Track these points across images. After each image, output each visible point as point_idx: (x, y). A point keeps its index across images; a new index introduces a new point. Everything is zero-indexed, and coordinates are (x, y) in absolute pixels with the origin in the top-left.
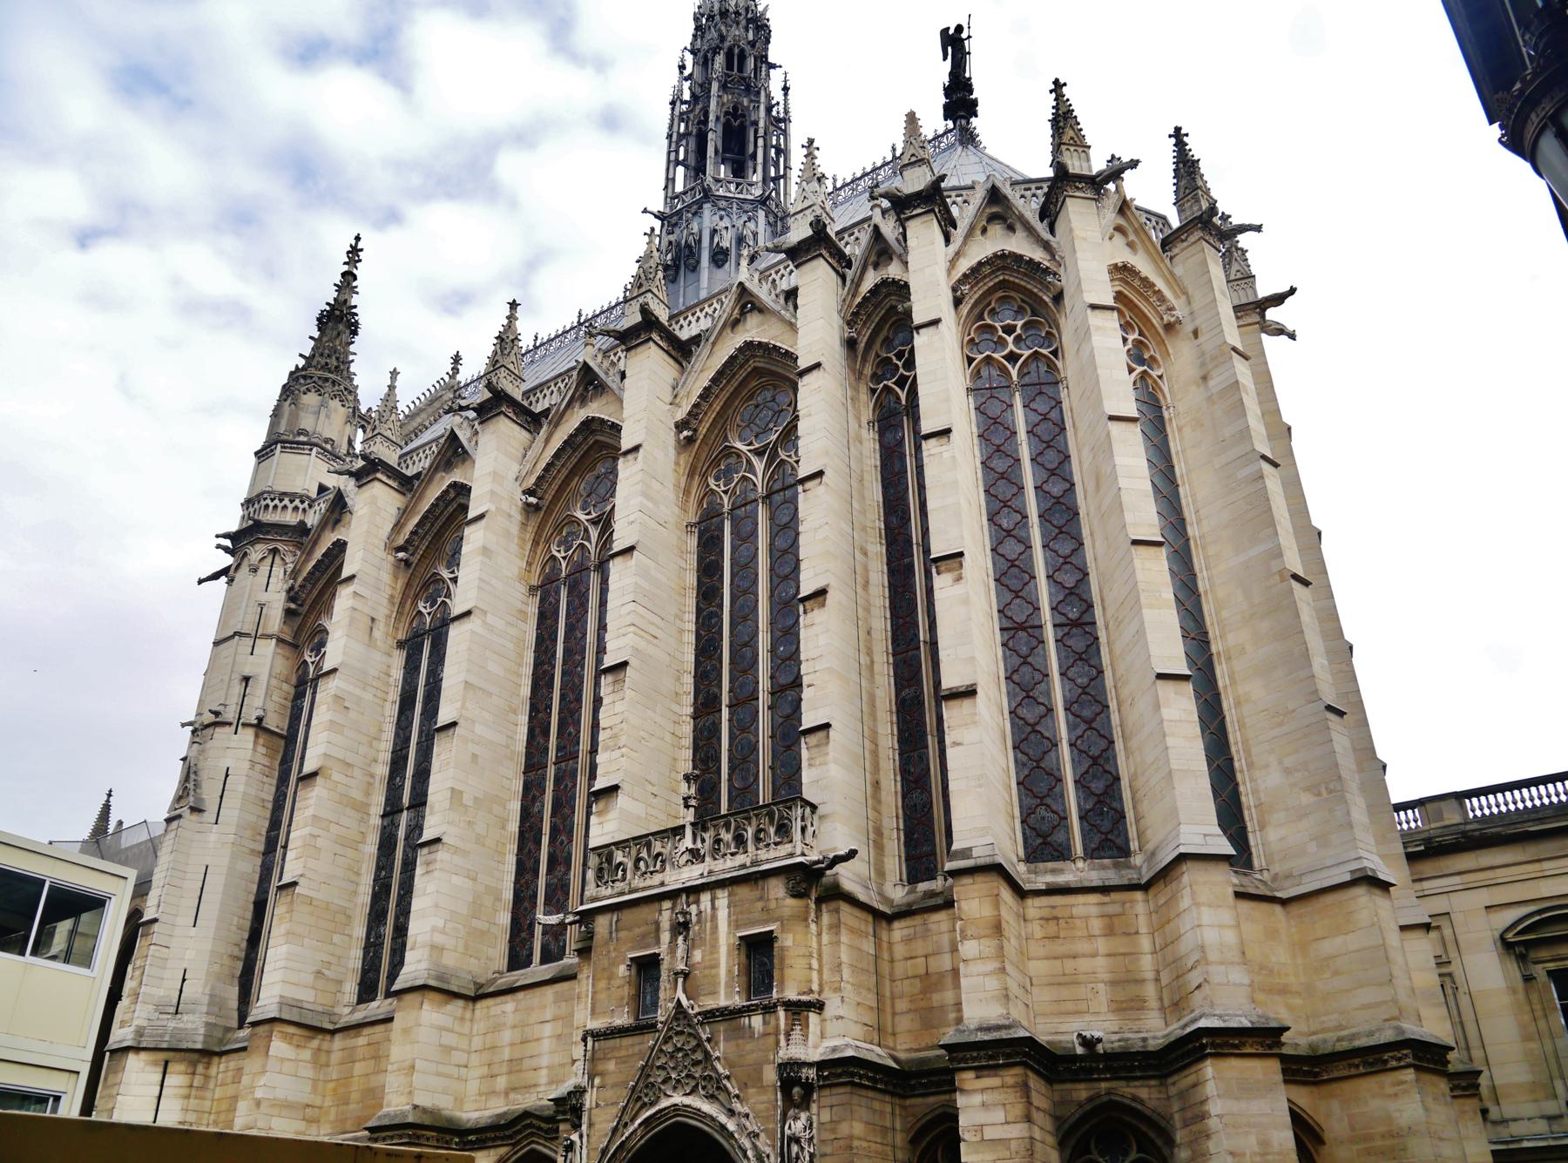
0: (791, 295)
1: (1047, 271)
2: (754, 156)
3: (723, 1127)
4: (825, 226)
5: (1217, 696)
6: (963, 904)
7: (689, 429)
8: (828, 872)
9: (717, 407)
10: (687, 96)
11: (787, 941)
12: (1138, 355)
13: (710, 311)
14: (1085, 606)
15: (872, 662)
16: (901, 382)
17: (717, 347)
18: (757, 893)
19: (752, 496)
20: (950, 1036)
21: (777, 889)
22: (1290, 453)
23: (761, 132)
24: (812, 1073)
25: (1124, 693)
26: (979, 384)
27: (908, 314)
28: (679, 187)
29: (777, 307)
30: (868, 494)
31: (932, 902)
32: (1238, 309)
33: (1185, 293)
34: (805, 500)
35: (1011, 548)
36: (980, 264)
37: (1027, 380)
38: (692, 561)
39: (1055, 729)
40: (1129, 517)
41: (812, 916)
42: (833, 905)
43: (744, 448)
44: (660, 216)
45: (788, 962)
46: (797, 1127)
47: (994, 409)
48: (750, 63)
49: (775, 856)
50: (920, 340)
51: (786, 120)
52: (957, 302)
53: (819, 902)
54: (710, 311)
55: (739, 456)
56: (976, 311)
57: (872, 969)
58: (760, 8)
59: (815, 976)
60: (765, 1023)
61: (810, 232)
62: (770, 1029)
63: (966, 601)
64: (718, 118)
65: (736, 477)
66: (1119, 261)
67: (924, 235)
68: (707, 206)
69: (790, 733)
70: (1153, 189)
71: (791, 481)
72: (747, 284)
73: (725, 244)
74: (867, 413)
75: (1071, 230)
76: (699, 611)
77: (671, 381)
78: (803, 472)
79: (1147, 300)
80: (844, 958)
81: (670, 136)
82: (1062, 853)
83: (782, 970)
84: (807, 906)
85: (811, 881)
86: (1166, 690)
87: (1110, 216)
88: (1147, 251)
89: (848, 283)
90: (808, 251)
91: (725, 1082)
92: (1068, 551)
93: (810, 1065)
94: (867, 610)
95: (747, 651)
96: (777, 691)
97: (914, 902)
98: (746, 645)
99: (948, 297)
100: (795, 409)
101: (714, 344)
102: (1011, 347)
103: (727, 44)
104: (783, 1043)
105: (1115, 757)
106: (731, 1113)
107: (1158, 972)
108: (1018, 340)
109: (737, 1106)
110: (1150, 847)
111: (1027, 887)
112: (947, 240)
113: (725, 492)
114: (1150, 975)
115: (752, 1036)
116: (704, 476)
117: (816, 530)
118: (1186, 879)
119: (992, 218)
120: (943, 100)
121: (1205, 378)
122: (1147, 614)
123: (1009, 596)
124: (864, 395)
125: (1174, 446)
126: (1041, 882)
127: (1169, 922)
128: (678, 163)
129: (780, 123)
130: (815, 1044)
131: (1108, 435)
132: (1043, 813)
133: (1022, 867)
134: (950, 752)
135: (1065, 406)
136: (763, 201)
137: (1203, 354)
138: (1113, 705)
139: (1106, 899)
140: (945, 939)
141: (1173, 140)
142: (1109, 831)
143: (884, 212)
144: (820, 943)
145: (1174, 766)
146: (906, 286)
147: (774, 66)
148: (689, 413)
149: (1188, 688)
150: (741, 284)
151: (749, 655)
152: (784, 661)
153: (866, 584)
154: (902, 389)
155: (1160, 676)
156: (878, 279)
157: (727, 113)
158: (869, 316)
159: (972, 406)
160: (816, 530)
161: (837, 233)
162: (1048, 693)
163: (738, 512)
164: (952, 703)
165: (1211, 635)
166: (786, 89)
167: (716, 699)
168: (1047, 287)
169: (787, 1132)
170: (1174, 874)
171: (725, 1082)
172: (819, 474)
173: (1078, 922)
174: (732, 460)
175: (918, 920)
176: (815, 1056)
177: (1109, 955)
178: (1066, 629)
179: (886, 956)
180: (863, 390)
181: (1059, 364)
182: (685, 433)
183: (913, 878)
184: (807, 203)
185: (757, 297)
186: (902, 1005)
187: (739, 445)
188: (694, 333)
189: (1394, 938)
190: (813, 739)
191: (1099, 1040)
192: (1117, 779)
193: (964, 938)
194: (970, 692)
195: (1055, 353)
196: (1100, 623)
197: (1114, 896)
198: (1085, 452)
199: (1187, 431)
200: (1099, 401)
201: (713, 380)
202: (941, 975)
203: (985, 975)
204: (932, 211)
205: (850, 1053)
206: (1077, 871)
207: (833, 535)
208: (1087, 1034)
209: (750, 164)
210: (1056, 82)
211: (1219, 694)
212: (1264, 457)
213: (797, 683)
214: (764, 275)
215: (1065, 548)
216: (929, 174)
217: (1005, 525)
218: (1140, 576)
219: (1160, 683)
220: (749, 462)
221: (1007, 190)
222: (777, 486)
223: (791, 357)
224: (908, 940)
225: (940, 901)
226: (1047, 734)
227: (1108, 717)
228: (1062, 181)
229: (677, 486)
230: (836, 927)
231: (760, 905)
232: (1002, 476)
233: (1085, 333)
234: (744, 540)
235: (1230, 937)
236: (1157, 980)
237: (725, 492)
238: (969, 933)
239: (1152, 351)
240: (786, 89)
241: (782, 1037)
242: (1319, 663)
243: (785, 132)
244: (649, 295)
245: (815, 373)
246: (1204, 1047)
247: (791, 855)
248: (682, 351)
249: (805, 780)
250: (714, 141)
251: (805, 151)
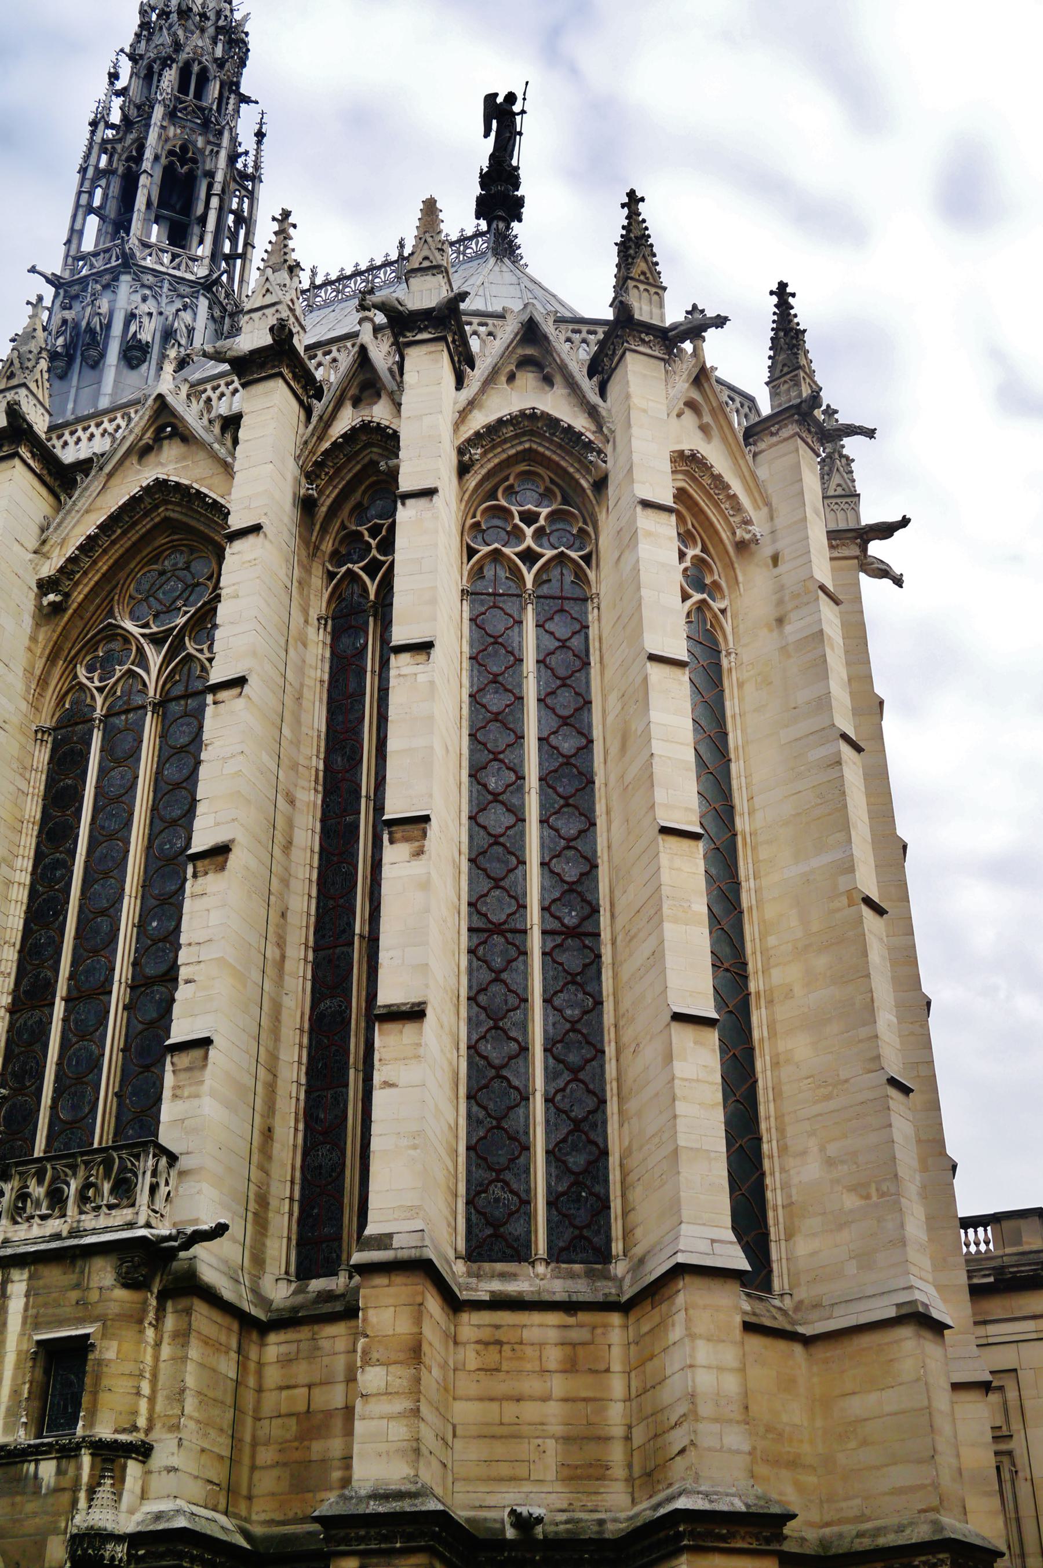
0: (232, 423)
1: (589, 446)
2: (203, 220)
4: (291, 334)
5: (749, 1052)
6: (371, 1313)
7: (57, 592)
8: (182, 1254)
9: (103, 566)
10: (115, 118)
11: (109, 1351)
12: (697, 578)
13: (110, 428)
14: (587, 910)
15: (283, 957)
16: (372, 569)
17: (113, 482)
18: (72, 1278)
19: (139, 701)
20: (329, 1504)
21: (103, 1274)
22: (878, 736)
23: (217, 188)
24: (120, 1551)
25: (627, 1036)
26: (480, 587)
27: (393, 474)
28: (88, 245)
29: (208, 438)
30: (305, 718)
31: (327, 1308)
32: (833, 536)
33: (768, 504)
34: (216, 715)
35: (497, 819)
36: (500, 422)
37: (545, 590)
38: (39, 781)
39: (527, 1077)
40: (660, 795)
41: (151, 1316)
42: (183, 1303)
43: (136, 631)
44: (54, 281)
45: (105, 1382)
47: (497, 624)
48: (214, 90)
49: (105, 1225)
50: (406, 514)
51: (255, 178)
52: (463, 470)
53: (163, 1297)
54: (110, 428)
55: (126, 641)
56: (488, 486)
57: (229, 1400)
58: (238, 16)
59: (143, 1405)
60: (60, 1472)
61: (267, 340)
62: (66, 1482)
63: (425, 885)
64: (157, 158)
65: (119, 670)
66: (686, 447)
67: (427, 370)
68: (125, 278)
69: (151, 1048)
70: (740, 359)
71: (199, 686)
72: (170, 399)
73: (145, 336)
74: (319, 605)
75: (628, 396)
76: (39, 856)
77: (39, 519)
78: (216, 676)
79: (717, 505)
80: (190, 1381)
81: (83, 170)
82: (519, 1252)
83: (95, 1394)
84: (145, 1302)
85: (158, 1269)
86: (683, 1036)
87: (682, 386)
88: (724, 439)
89: (314, 420)
90: (262, 366)
92: (573, 832)
93: (119, 1538)
94: (285, 882)
95: (104, 923)
96: (138, 985)
97: (301, 1307)
98: (103, 912)
99: (449, 461)
100: (217, 586)
101: (110, 475)
102: (529, 542)
103: (183, 56)
104: (82, 1503)
105: (605, 1122)
107: (630, 1427)
108: (539, 534)
110: (638, 1251)
111: (464, 1295)
112: (460, 384)
113: (100, 690)
114: (619, 1431)
115: (37, 1491)
116: (72, 663)
117: (225, 760)
118: (680, 1299)
119: (525, 363)
120: (478, 191)
121: (780, 621)
122: (670, 930)
123: (485, 885)
124: (317, 580)
125: (731, 707)
126: (485, 1289)
127: (651, 1358)
128: (90, 210)
129: (246, 181)
131: (645, 679)
132: (498, 1192)
133: (460, 1267)
134: (379, 1096)
135: (593, 632)
136: (208, 285)
137: (782, 588)
138: (610, 1050)
139: (571, 1320)
140: (340, 1363)
141: (775, 299)
142: (585, 1227)
143: (377, 330)
144: (156, 1358)
145: (682, 1142)
146: (395, 436)
147: (247, 100)
148: (61, 570)
149: (713, 1037)
150: (160, 397)
151: (105, 927)
152: (155, 942)
153: (288, 846)
154: (373, 579)
155: (678, 1017)
156: (357, 422)
157: (171, 153)
158: (338, 471)
159: (466, 615)
160: (225, 760)
161: (308, 348)
162: (524, 1026)
163: (116, 721)
164: (389, 1027)
165: (751, 967)
166: (260, 135)
167: (50, 987)
168: (586, 467)
170: (667, 1292)
172: (240, 682)
173: (529, 1351)
174: (116, 645)
175: (304, 1333)
176: (128, 1524)
177: (566, 1400)
178: (559, 940)
179: (252, 1382)
180: (317, 571)
181: (591, 575)
182: (51, 597)
183: (305, 1270)
184: (269, 299)
185: (182, 419)
186: (266, 1455)
187: (129, 625)
188: (83, 455)
189: (942, 1399)
190: (184, 1060)
191: (539, 1520)
192: (605, 1153)
193: (367, 1362)
194: (414, 1014)
195: (587, 559)
196: (605, 935)
197: (583, 1317)
198: (613, 699)
199: (749, 688)
200: (638, 633)
201: (105, 528)
202: (329, 1414)
203: (390, 1418)
204: (444, 339)
205: (181, 1523)
206: (535, 1279)
207: (247, 771)
208: (523, 1510)
209: (196, 230)
210: (631, 194)
211: (753, 1049)
212: (845, 737)
213: (170, 977)
214: (195, 389)
215: (570, 827)
216: (445, 287)
217: (492, 786)
218: (666, 877)
219: (675, 1026)
220: (140, 650)
221: (548, 327)
222: (178, 690)
223: (220, 511)
224: (286, 1361)
225: (339, 1307)
226: (516, 1082)
227: (602, 1067)
228: (623, 330)
229: (29, 671)
230: (182, 1336)
231: (74, 1295)
232: (496, 717)
233: (629, 539)
234: (119, 762)
235: (731, 1384)
236: (628, 1438)
237: (100, 690)
238: (375, 1356)
239: (716, 575)
240: (260, 135)
241: (82, 1495)
242: (886, 1020)
243: (251, 195)
244: (23, 391)
245: (251, 539)
246: (680, 1536)
247: (131, 1225)
248: (61, 479)
249: (164, 1117)
250: (147, 188)
251: (276, 226)
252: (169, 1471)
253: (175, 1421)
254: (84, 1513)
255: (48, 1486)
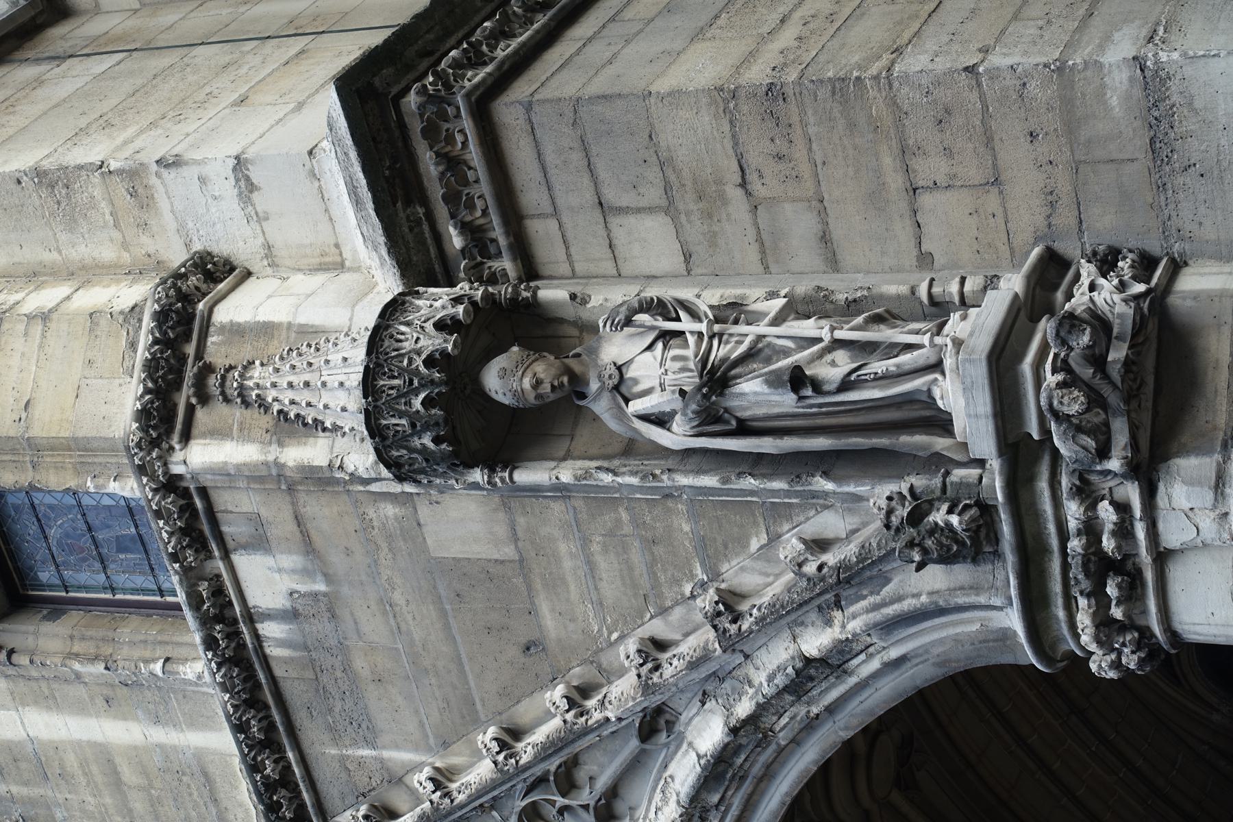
3: (718, 770)
46: (654, 374)
60: (260, 543)
62: (277, 514)
91: (526, 750)
106: (655, 724)
109: (622, 694)
115: (329, 606)
130: (322, 287)
169: (677, 437)
171: (526, 750)
252: (252, 187)
253: (120, 188)
254: (341, 443)
255: (306, 573)
